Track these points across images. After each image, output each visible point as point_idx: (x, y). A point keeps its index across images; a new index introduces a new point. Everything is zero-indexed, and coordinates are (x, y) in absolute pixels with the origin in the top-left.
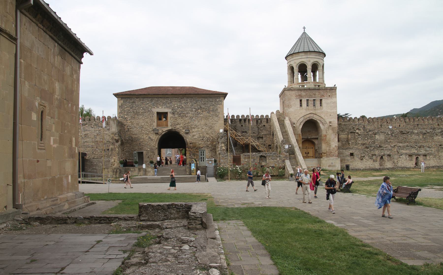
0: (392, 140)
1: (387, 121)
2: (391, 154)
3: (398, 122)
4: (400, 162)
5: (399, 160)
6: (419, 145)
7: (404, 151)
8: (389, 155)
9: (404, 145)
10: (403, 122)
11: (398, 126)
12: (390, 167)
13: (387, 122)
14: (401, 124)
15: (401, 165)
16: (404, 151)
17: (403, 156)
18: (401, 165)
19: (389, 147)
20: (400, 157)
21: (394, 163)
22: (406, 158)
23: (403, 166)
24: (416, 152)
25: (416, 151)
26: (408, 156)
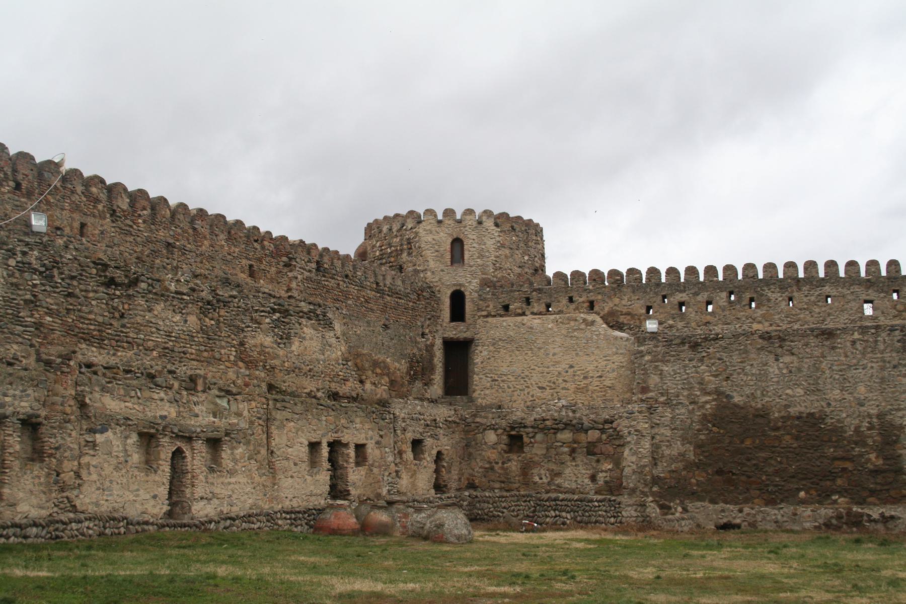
0: (50, 313)
1: (20, 177)
2: (43, 413)
3: (75, 198)
4: (94, 477)
5: (88, 464)
6: (184, 370)
7: (112, 405)
8: (31, 425)
9: (113, 361)
10: (100, 207)
11: (76, 225)
12: (34, 513)
13: (18, 186)
14: (89, 220)
15: (97, 504)
16: (112, 405)
17: (109, 434)
18: (97, 504)
19: (31, 361)
20: (94, 445)
21: (56, 482)
22: (126, 451)
23: (105, 508)
24: (174, 415)
25: (171, 411)
26: (134, 438)
